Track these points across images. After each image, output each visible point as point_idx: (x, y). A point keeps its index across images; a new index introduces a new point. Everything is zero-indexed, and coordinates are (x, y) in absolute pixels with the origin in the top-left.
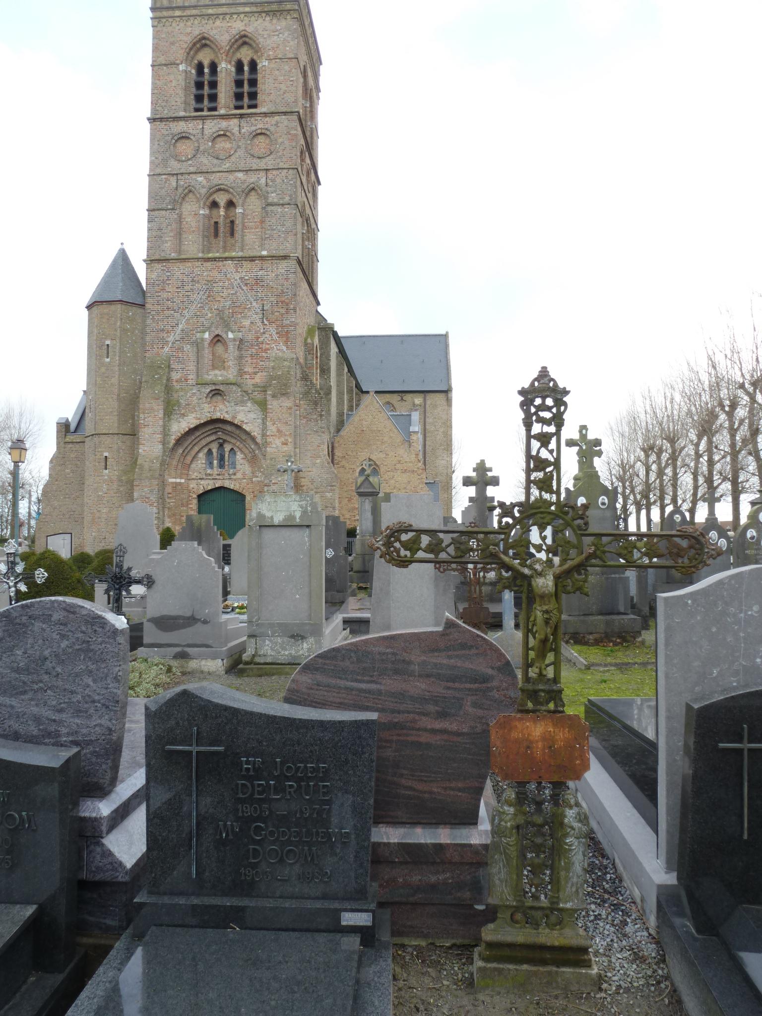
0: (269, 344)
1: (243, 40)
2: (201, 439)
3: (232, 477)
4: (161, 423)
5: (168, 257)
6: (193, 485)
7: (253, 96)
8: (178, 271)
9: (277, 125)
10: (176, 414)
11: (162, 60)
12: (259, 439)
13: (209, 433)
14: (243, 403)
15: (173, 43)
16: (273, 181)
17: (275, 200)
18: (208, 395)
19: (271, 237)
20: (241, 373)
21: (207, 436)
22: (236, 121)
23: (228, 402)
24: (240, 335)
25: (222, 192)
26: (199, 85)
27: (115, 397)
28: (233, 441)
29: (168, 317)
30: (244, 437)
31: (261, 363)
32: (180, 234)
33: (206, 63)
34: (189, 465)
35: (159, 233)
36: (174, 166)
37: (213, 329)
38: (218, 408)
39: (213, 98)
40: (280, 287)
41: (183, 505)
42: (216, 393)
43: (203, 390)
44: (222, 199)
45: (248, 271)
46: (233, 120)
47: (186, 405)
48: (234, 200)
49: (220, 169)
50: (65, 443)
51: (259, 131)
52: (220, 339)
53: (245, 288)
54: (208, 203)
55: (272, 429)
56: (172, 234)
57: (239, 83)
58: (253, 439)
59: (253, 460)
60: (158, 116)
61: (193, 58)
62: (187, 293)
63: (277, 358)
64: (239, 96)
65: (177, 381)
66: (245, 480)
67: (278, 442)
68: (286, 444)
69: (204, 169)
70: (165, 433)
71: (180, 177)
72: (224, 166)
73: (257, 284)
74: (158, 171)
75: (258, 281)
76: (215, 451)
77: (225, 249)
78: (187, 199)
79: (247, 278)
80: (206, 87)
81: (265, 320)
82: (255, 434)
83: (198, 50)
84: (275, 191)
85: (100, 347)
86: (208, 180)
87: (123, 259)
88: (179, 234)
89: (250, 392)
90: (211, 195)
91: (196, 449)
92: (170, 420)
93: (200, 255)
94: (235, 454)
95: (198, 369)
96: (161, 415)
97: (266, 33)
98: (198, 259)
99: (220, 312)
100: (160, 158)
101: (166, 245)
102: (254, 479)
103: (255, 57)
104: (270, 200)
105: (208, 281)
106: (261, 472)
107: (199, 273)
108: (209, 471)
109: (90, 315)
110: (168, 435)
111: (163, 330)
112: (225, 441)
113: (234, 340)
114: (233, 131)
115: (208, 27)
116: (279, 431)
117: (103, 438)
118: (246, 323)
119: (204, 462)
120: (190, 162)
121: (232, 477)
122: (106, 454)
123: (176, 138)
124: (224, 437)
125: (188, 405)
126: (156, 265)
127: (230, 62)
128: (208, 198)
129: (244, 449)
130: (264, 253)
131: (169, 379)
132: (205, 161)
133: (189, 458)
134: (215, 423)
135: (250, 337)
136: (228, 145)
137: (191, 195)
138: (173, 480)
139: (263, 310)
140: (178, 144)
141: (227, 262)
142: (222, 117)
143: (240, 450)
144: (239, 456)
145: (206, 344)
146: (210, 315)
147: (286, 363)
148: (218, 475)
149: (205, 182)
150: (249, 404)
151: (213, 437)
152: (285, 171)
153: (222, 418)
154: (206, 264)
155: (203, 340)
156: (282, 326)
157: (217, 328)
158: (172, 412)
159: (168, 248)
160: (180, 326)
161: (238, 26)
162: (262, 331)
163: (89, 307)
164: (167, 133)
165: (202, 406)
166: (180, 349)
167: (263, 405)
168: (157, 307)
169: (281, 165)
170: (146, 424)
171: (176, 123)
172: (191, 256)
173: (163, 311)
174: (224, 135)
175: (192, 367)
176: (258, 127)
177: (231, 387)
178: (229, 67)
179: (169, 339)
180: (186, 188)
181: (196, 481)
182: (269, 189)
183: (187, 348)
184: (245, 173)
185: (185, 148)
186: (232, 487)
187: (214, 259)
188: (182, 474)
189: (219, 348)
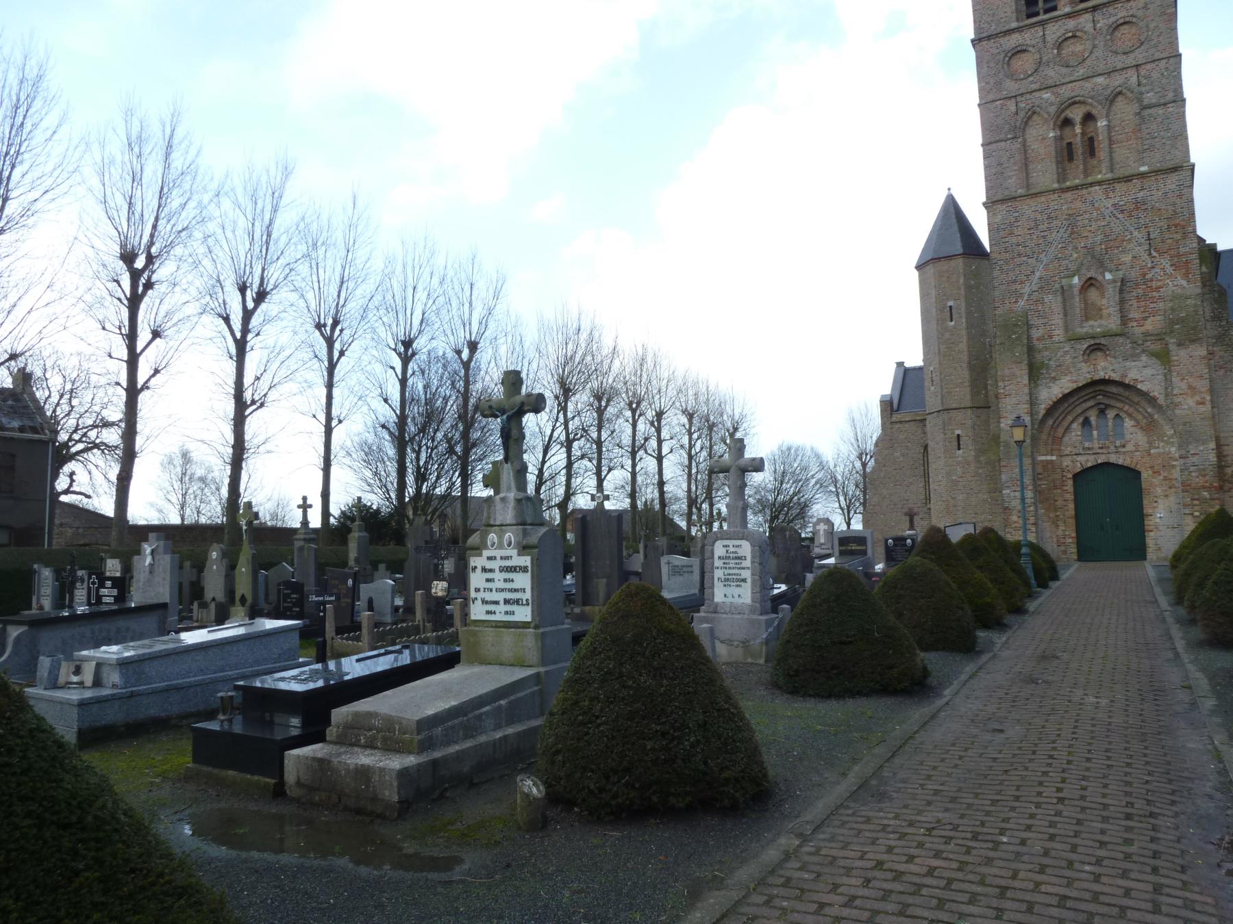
2: (1076, 407)
3: (1120, 449)
4: (1026, 390)
5: (1014, 194)
6: (1066, 462)
8: (1029, 209)
10: (1045, 378)
12: (1161, 400)
13: (1086, 398)
14: (1134, 357)
16: (1148, 77)
17: (1154, 101)
18: (1085, 351)
20: (1125, 320)
21: (1083, 402)
22: (1088, 16)
23: (1115, 357)
24: (1120, 274)
25: (1077, 106)
27: (965, 365)
28: (1119, 405)
30: (1136, 399)
31: (1152, 305)
32: (1026, 165)
36: (1011, 86)
37: (1084, 271)
38: (1099, 367)
40: (1171, 208)
41: (1055, 487)
42: (1096, 348)
43: (1078, 346)
44: (1076, 114)
45: (1123, 195)
46: (1083, 15)
47: (1057, 366)
48: (1094, 112)
49: (1072, 78)
50: (892, 423)
51: (1122, 21)
52: (1094, 282)
53: (1120, 216)
54: (1059, 123)
55: (1180, 385)
56: (1016, 168)
58: (1152, 401)
59: (1150, 427)
60: (984, 35)
62: (1042, 234)
63: (1174, 297)
65: (1038, 340)
66: (1138, 453)
67: (1191, 402)
68: (1203, 403)
69: (1050, 82)
70: (1033, 402)
71: (1019, 99)
72: (1077, 74)
73: (1137, 209)
74: (991, 97)
75: (1138, 204)
76: (1093, 419)
77: (1086, 175)
78: (1030, 123)
79: (1122, 203)
81: (1152, 252)
82: (1156, 394)
84: (1152, 90)
85: (942, 311)
86: (1057, 95)
88: (1026, 164)
89: (1140, 342)
90: (1063, 111)
92: (1037, 386)
93: (1056, 186)
94: (1122, 419)
95: (1065, 322)
96: (1026, 381)
98: (1054, 191)
100: (992, 82)
101: (1010, 181)
102: (1152, 451)
104: (1146, 102)
105: (1069, 215)
106: (1163, 441)
107: (1056, 207)
108: (1087, 445)
109: (920, 276)
110: (1036, 404)
111: (1015, 282)
112: (1108, 406)
113: (1114, 281)
114: (1085, 29)
116: (1190, 387)
118: (1127, 258)
119: (1079, 433)
120: (1031, 79)
121: (1120, 449)
122: (958, 432)
123: (1010, 54)
124: (1107, 401)
125: (1060, 366)
126: (999, 206)
128: (1058, 117)
129: (1135, 414)
130: (1144, 169)
131: (1029, 338)
132: (1052, 73)
133: (1061, 430)
134: (1097, 386)
135: (1134, 274)
136: (1079, 48)
137: (1035, 117)
138: (1043, 458)
139: (1149, 239)
140: (1013, 62)
141: (1093, 189)
142: (1068, 16)
143: (1130, 415)
144: (1128, 423)
145: (1076, 291)
146: (1076, 255)
147: (1189, 302)
148: (1099, 448)
149: (1053, 98)
150: (1144, 358)
151: (1091, 403)
152: (1164, 62)
153: (1107, 377)
154: (1064, 196)
155: (1071, 286)
156: (1179, 255)
157: (1088, 269)
158: (1038, 377)
159: (1013, 183)
160: (1038, 274)
162: (1149, 265)
163: (918, 267)
165: (1079, 365)
166: (1040, 301)
167: (1163, 357)
168: (1004, 256)
169: (1158, 55)
170: (1007, 393)
171: (1008, 38)
172: (1044, 189)
173: (1013, 259)
174: (1074, 36)
175: (1057, 320)
176: (1119, 16)
177: (1117, 338)
179: (1024, 291)
180: (1029, 110)
181: (1070, 458)
182: (1143, 89)
183: (1048, 298)
184: (1106, 76)
185: (1025, 63)
186: (1120, 462)
187: (1076, 188)
189: (1093, 294)
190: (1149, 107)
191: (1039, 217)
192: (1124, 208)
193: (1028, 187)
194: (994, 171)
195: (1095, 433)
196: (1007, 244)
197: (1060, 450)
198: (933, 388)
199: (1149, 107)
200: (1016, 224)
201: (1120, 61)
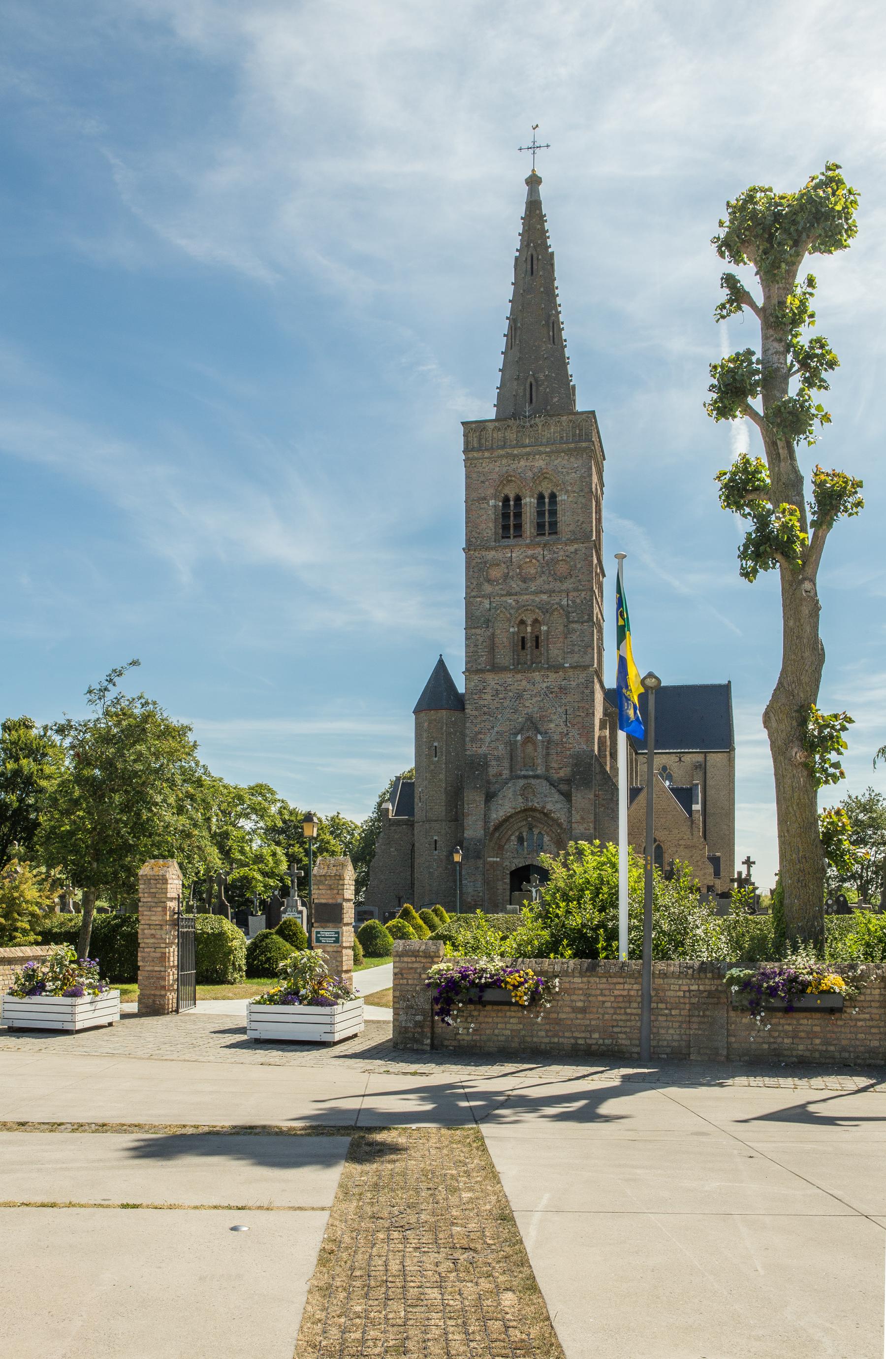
0: (571, 744)
1: (541, 476)
4: (482, 812)
7: (554, 525)
8: (492, 680)
11: (474, 495)
19: (572, 652)
26: (506, 516)
27: (443, 790)
29: (484, 721)
33: (512, 496)
35: (475, 649)
39: (518, 527)
51: (561, 558)
55: (576, 817)
57: (540, 514)
58: (560, 825)
64: (540, 526)
68: (589, 829)
70: (486, 819)
80: (512, 518)
84: (575, 611)
85: (430, 748)
86: (517, 602)
94: (543, 835)
97: (565, 470)
100: (475, 583)
103: (555, 490)
104: (571, 619)
122: (436, 838)
135: (556, 737)
138: (491, 859)
143: (548, 834)
149: (514, 603)
151: (524, 823)
155: (516, 741)
161: (540, 463)
164: (480, 561)
167: (567, 796)
168: (475, 713)
178: (532, 500)
182: (570, 609)
188: (497, 854)
189: (530, 748)
190: (573, 622)
191: (499, 688)
192: (553, 690)
194: (472, 649)
195: (525, 843)
196: (477, 705)
197: (502, 854)
198: (420, 804)
200: (485, 691)
201: (557, 585)
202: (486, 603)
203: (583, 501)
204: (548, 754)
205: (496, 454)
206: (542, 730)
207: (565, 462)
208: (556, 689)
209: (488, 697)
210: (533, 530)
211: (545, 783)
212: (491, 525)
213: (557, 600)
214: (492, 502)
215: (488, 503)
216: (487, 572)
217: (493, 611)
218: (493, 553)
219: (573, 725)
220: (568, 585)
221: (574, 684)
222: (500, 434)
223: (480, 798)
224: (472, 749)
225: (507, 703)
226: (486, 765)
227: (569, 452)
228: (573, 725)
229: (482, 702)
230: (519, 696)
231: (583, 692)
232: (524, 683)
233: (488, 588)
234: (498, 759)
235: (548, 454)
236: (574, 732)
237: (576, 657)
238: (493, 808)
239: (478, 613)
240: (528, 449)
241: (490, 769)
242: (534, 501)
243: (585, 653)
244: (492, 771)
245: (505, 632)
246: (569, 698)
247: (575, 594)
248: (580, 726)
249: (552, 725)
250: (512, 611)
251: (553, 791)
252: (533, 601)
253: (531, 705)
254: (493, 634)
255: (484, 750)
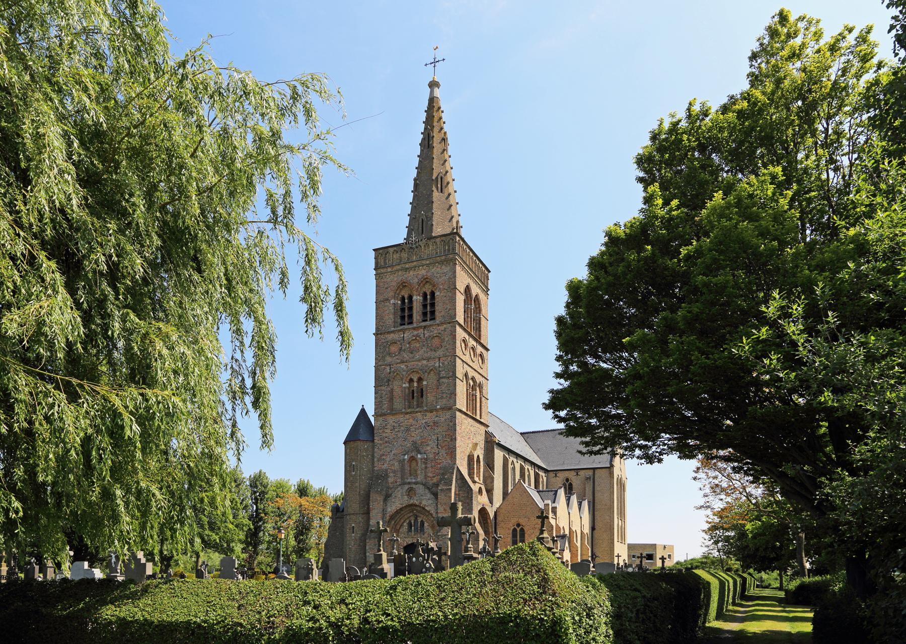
1: (426, 281)
4: (381, 507)
7: (433, 312)
8: (391, 420)
9: (445, 330)
11: (381, 298)
15: (387, 288)
19: (442, 398)
20: (426, 477)
22: (422, 330)
26: (403, 310)
33: (406, 296)
34: (399, 530)
39: (411, 316)
57: (425, 306)
58: (431, 515)
61: (398, 294)
64: (425, 314)
70: (384, 511)
80: (406, 311)
83: (401, 290)
87: (363, 412)
88: (391, 399)
91: (402, 521)
99: (414, 443)
104: (441, 375)
115: (405, 276)
117: (352, 516)
127: (419, 295)
133: (398, 527)
135: (431, 456)
142: (414, 329)
155: (404, 460)
161: (422, 272)
163: (345, 443)
168: (381, 442)
189: (414, 464)
190: (442, 378)
193: (392, 410)
194: (378, 400)
199: (442, 378)
201: (433, 354)
202: (388, 368)
203: (450, 295)
204: (426, 468)
205: (395, 268)
206: (422, 451)
207: (439, 269)
208: (432, 424)
209: (389, 431)
210: (418, 318)
211: (421, 486)
212: (392, 316)
213: (433, 364)
214: (392, 301)
215: (390, 303)
216: (389, 348)
217: (392, 374)
218: (392, 335)
219: (442, 447)
220: (440, 353)
221: (443, 419)
222: (398, 255)
223: (380, 499)
224: (378, 466)
225: (400, 434)
226: (387, 476)
227: (441, 263)
228: (442, 447)
229: (384, 435)
230: (408, 430)
231: (448, 425)
232: (411, 420)
233: (388, 359)
234: (394, 472)
235: (428, 265)
236: (443, 452)
237: (444, 401)
238: (389, 504)
239: (383, 376)
240: (415, 263)
241: (389, 479)
242: (420, 298)
243: (450, 398)
244: (390, 480)
245: (400, 387)
246: (440, 429)
247: (444, 359)
248: (447, 447)
249: (429, 448)
250: (404, 373)
251: (427, 491)
252: (417, 365)
253: (415, 436)
254: (392, 389)
255: (385, 466)
